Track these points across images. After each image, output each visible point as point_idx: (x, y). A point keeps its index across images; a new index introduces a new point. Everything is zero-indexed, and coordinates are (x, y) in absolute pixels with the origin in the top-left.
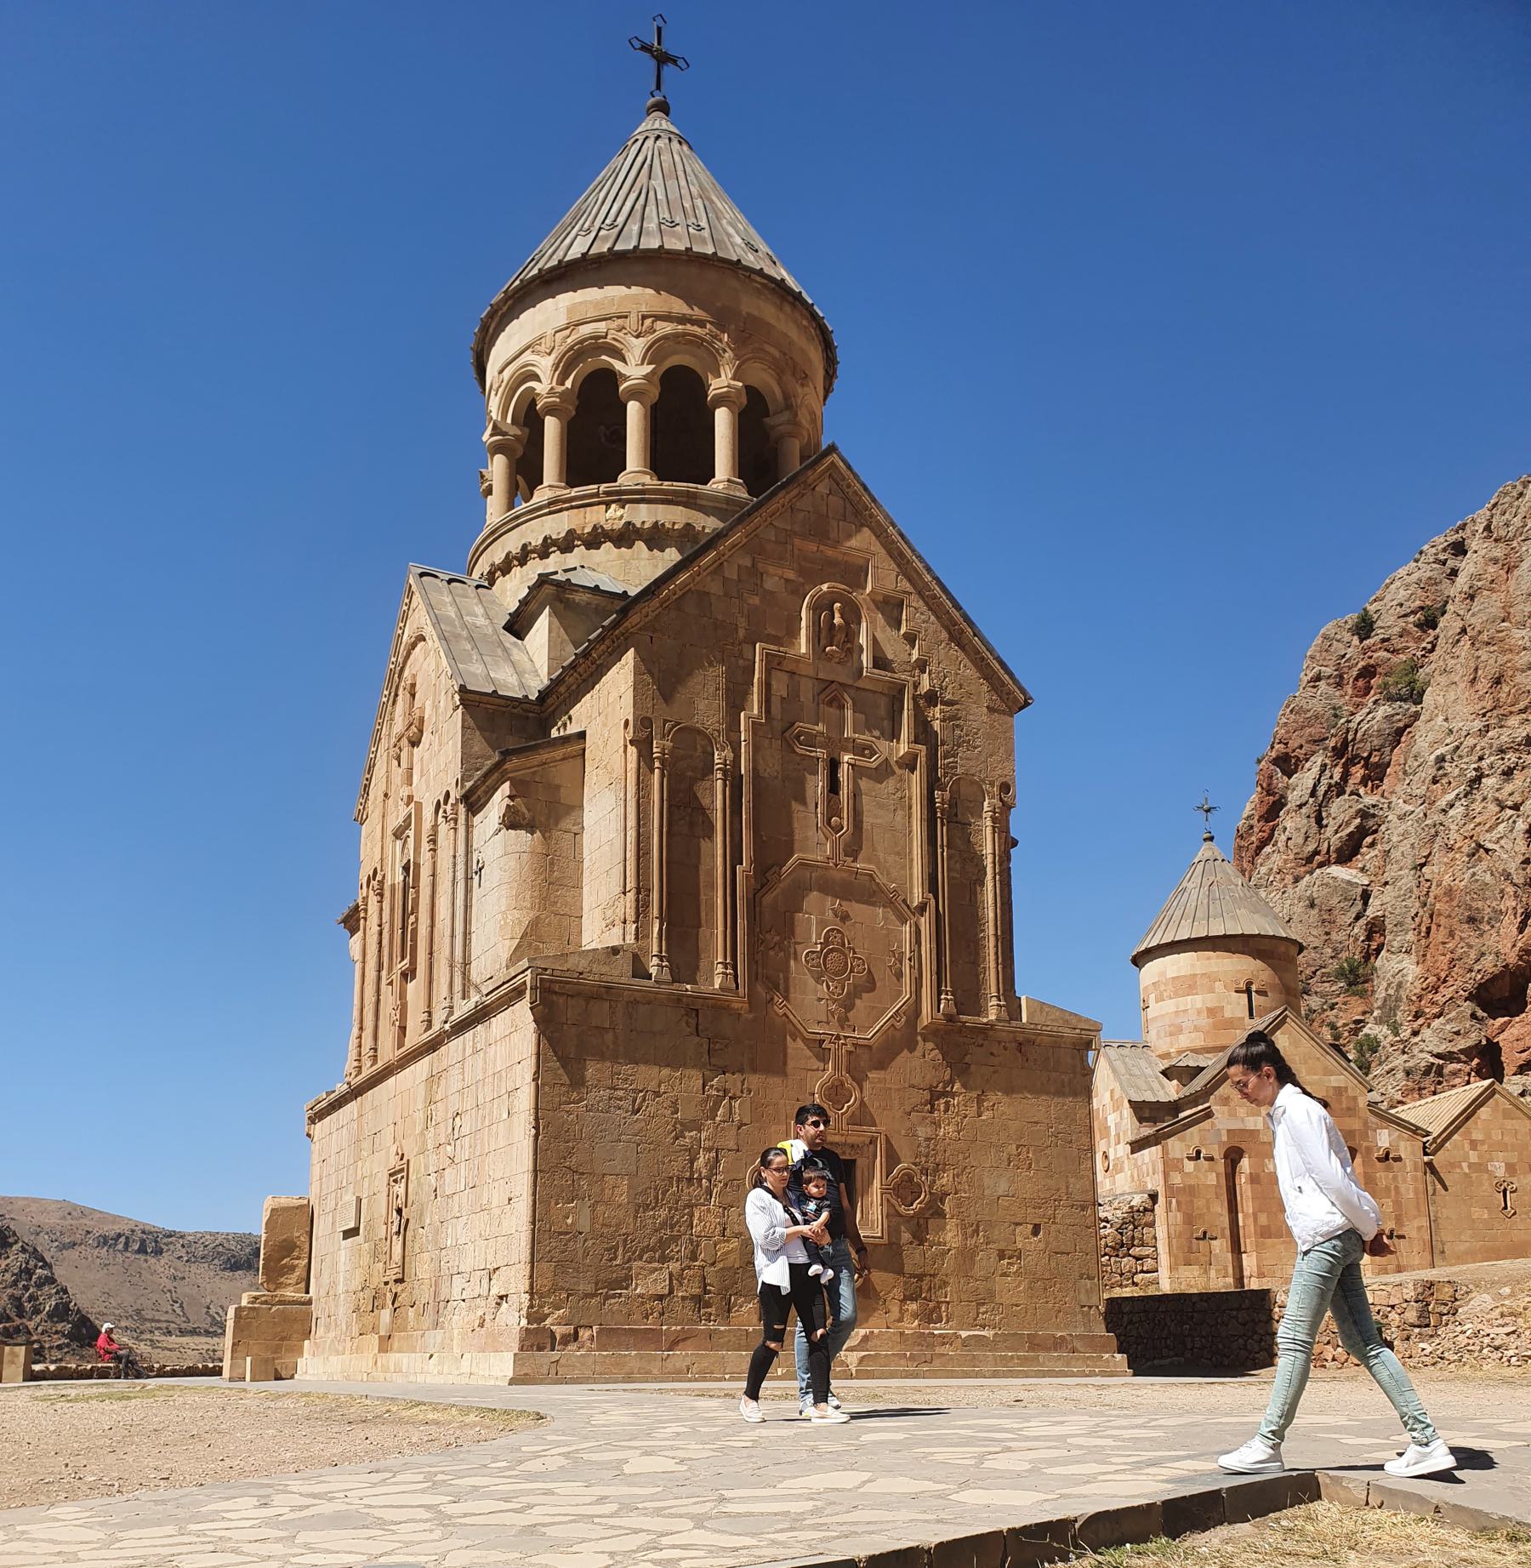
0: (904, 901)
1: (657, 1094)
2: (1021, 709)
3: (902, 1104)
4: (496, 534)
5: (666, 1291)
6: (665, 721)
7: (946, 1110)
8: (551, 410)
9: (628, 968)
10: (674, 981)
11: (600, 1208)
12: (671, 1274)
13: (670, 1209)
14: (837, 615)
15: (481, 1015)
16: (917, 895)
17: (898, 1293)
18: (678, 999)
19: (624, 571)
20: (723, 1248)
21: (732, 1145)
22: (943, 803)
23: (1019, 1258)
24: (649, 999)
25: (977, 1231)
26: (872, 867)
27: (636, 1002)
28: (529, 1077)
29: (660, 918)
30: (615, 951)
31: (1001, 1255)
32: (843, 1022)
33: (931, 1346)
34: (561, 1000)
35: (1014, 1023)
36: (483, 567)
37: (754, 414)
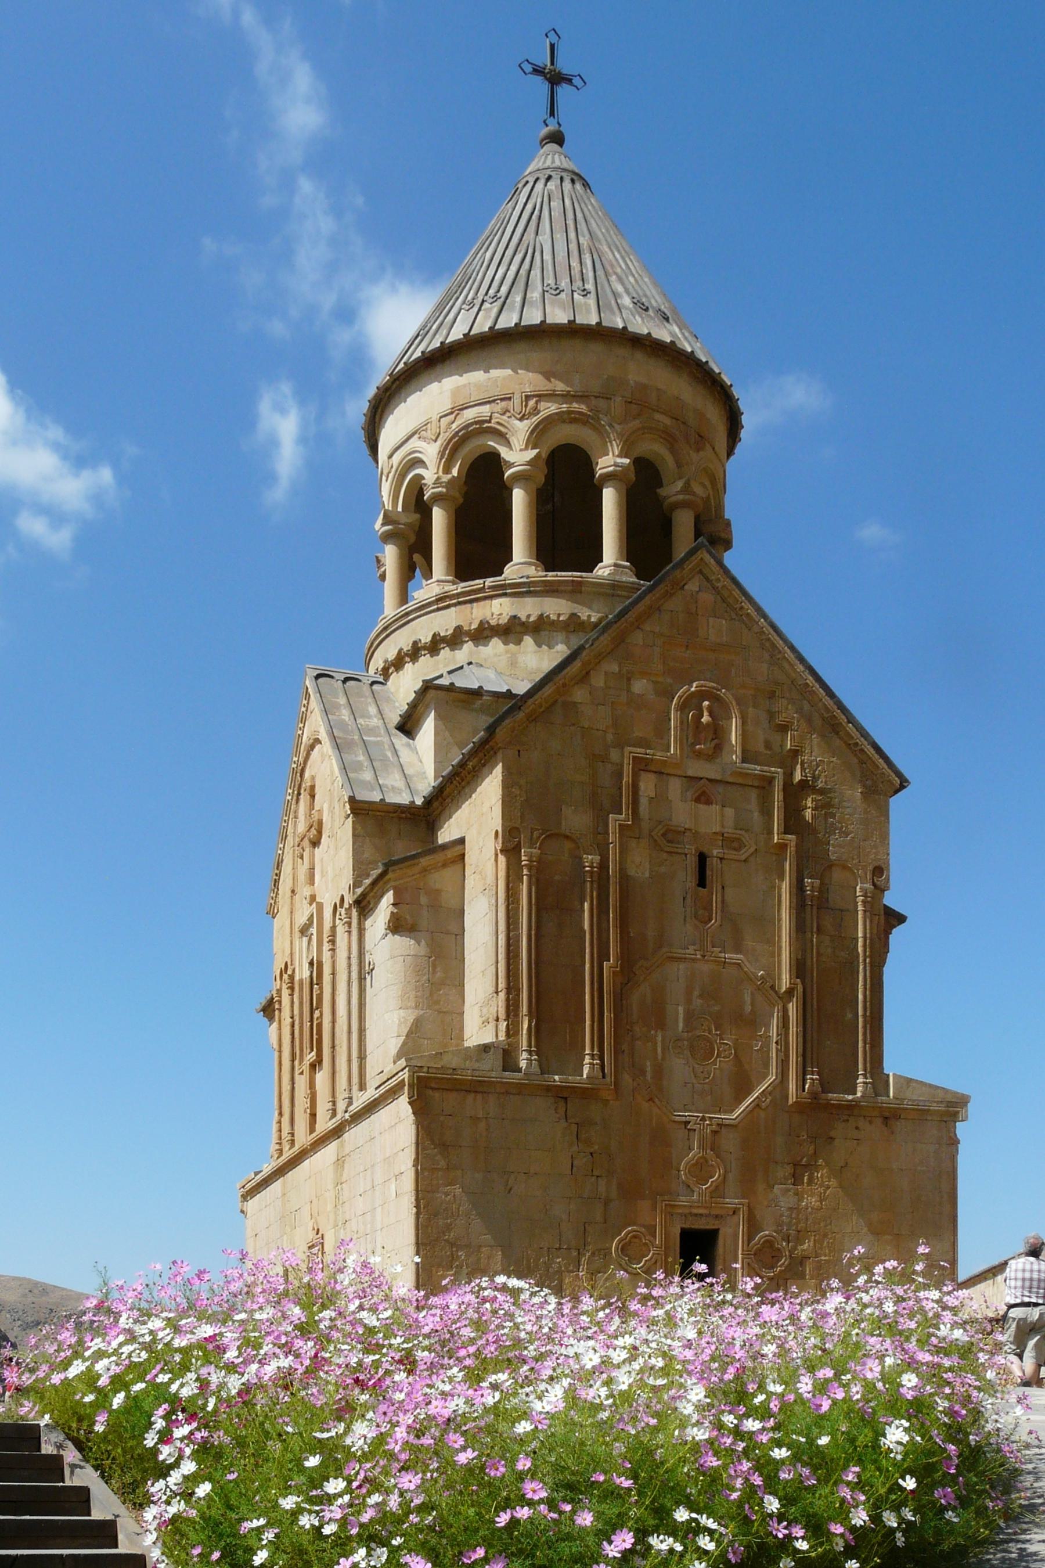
0: (772, 987)
2: (896, 792)
4: (388, 631)
8: (437, 498)
9: (499, 1063)
14: (706, 713)
15: (371, 1108)
16: (785, 981)
18: (548, 1089)
19: (512, 668)
24: (520, 1089)
28: (410, 1163)
29: (530, 1014)
30: (486, 1048)
34: (437, 1095)
36: (377, 662)
37: (643, 487)
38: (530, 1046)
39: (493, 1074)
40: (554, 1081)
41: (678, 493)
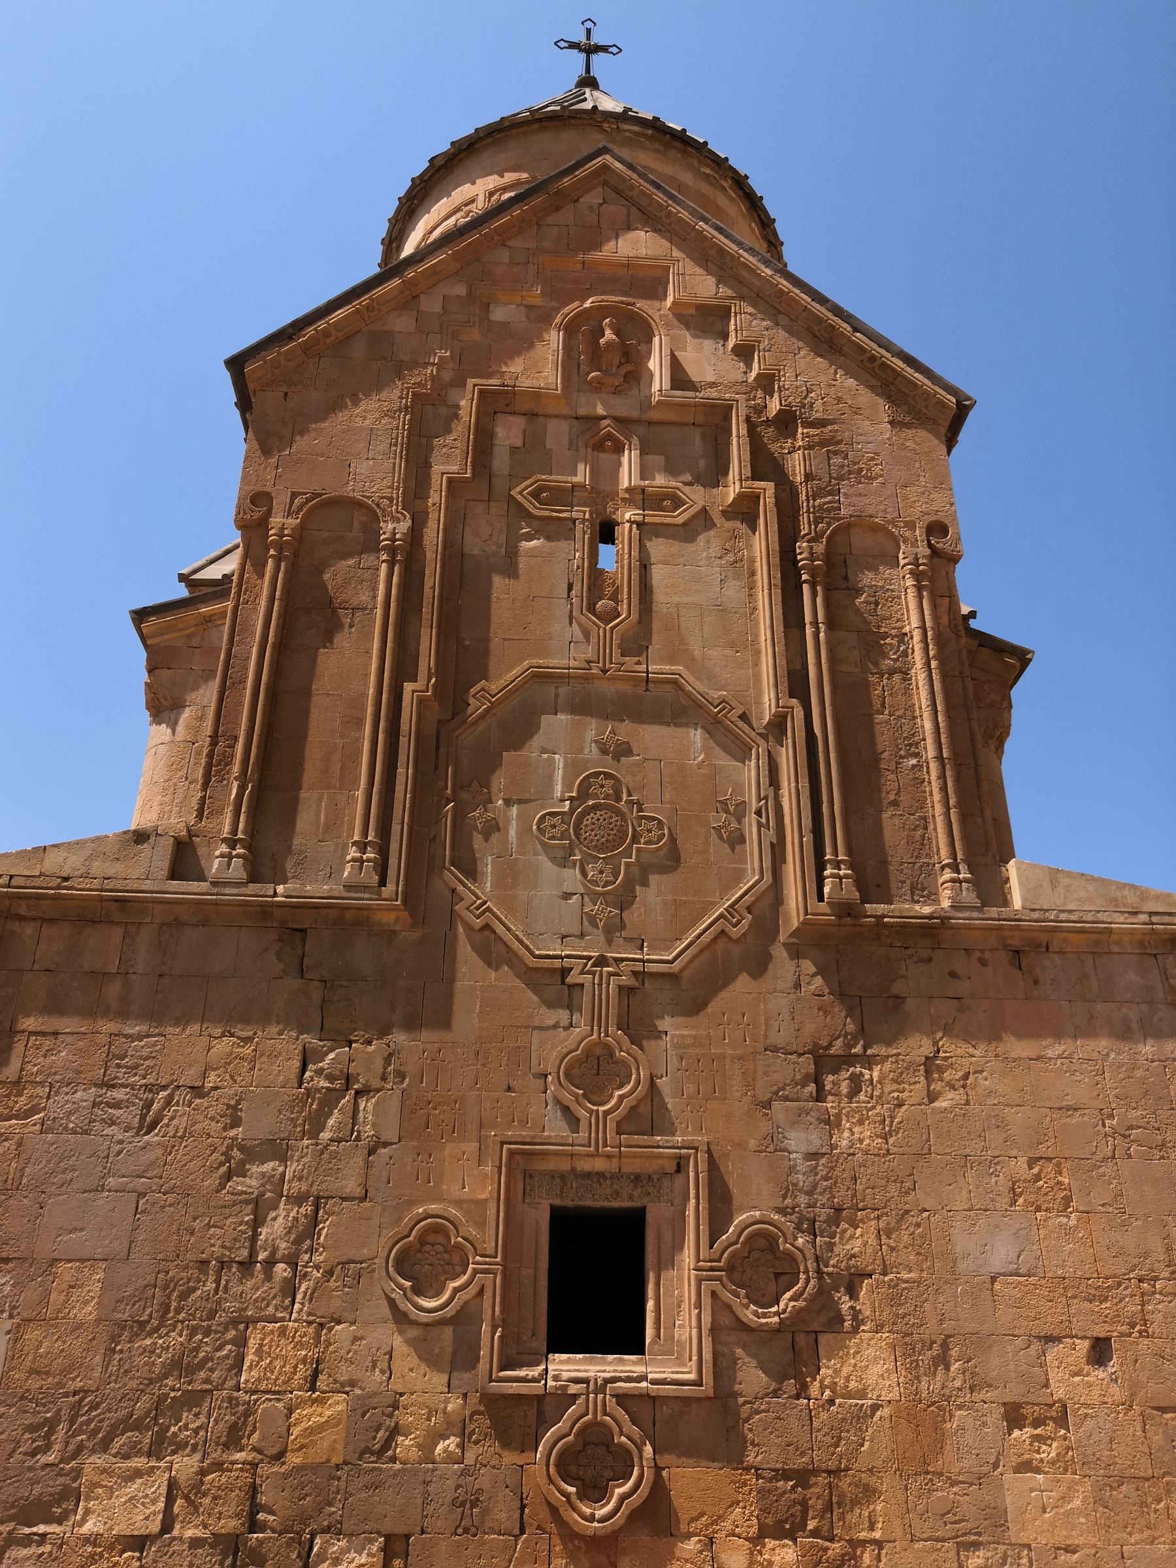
0: (744, 717)
1: (197, 1091)
3: (750, 1085)
5: (155, 1527)
6: (294, 496)
7: (855, 1091)
11: (32, 1335)
12: (172, 1484)
13: (194, 1331)
16: (768, 703)
17: (743, 1517)
18: (264, 912)
20: (309, 1417)
21: (351, 1186)
22: (812, 557)
23: (1062, 1420)
24: (204, 915)
25: (943, 1360)
27: (179, 924)
30: (140, 837)
31: (1014, 1416)
32: (614, 929)
34: (29, 929)
35: (993, 911)
38: (234, 831)
39: (147, 885)
40: (275, 894)
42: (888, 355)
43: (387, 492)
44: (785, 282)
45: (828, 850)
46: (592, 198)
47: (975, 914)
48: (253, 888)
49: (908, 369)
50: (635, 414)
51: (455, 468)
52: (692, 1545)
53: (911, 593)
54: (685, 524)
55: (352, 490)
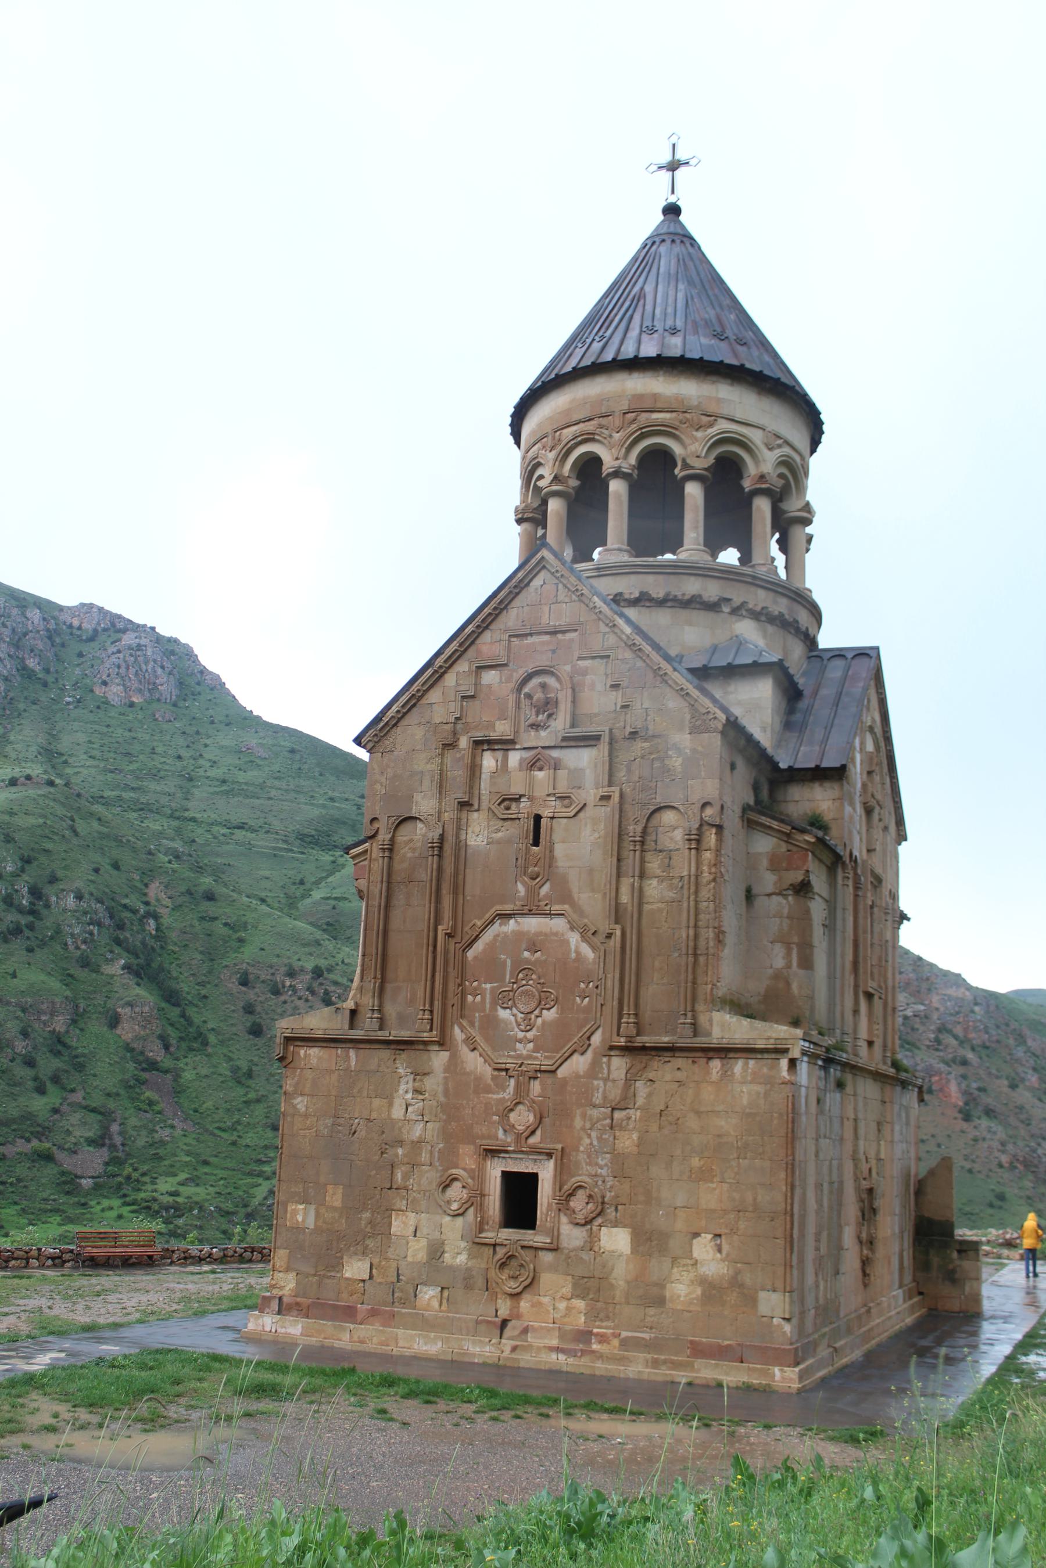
5: (366, 1277)
10: (381, 1029)
12: (371, 1265)
26: (566, 907)
33: (589, 1342)
41: (681, 470)
42: (690, 687)
43: (432, 811)
44: (638, 637)
45: (625, 1008)
46: (537, 582)
47: (689, 1041)
48: (380, 1033)
49: (701, 697)
50: (553, 744)
51: (459, 795)
52: (545, 1300)
53: (687, 851)
54: (575, 816)
55: (414, 813)
